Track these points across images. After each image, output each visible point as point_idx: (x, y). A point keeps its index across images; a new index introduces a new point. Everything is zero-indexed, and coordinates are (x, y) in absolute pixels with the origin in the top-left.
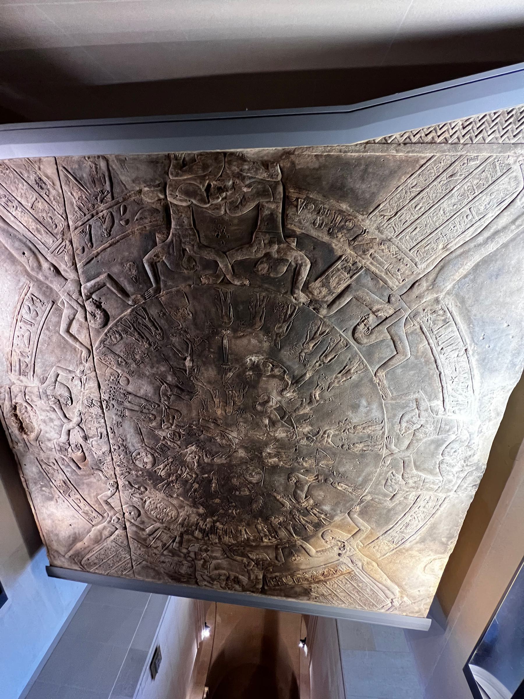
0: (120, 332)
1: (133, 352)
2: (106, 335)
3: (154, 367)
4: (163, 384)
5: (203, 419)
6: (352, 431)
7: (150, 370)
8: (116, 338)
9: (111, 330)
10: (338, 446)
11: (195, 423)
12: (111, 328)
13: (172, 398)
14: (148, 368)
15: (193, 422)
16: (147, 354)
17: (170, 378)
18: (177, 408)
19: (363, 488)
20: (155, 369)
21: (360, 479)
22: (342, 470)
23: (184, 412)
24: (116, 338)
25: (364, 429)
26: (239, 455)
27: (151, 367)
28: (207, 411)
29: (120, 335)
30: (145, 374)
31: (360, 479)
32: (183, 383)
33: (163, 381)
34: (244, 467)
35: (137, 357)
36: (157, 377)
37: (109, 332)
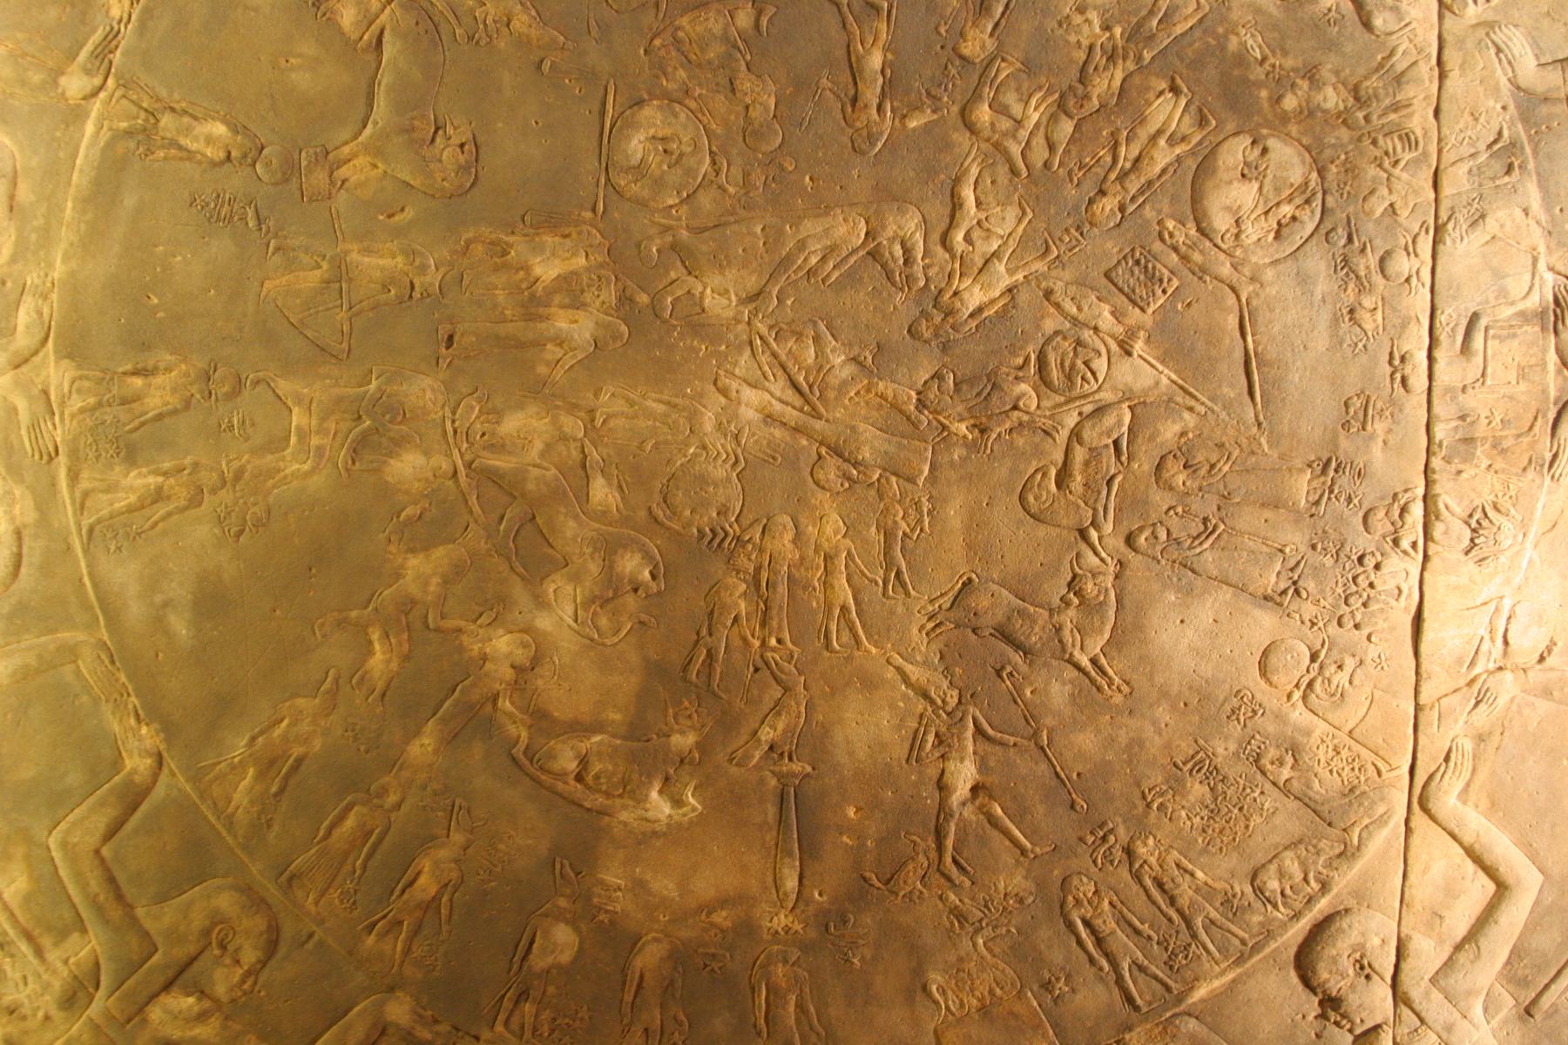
0: (1258, 905)
1: (1214, 814)
2: (1325, 887)
3: (1129, 746)
4: (1094, 661)
5: (911, 480)
6: (208, 478)
7: (1149, 731)
8: (1281, 874)
9: (1298, 906)
10: (257, 383)
11: (957, 453)
12: (1297, 916)
13: (1056, 589)
14: (1155, 743)
15: (964, 460)
16: (1148, 806)
17: (1057, 691)
18: (1042, 531)
19: (110, 145)
20: (1123, 737)
21: (130, 201)
22: (221, 246)
23: (1004, 518)
24: (1281, 874)
25: (159, 489)
26: (731, 274)
27: (1141, 744)
28: (889, 536)
29: (1259, 891)
30: (1174, 707)
31: (130, 201)
32: (998, 673)
33: (1091, 678)
34: (706, 200)
35: (1197, 790)
36: (1118, 699)
37: (1310, 900)
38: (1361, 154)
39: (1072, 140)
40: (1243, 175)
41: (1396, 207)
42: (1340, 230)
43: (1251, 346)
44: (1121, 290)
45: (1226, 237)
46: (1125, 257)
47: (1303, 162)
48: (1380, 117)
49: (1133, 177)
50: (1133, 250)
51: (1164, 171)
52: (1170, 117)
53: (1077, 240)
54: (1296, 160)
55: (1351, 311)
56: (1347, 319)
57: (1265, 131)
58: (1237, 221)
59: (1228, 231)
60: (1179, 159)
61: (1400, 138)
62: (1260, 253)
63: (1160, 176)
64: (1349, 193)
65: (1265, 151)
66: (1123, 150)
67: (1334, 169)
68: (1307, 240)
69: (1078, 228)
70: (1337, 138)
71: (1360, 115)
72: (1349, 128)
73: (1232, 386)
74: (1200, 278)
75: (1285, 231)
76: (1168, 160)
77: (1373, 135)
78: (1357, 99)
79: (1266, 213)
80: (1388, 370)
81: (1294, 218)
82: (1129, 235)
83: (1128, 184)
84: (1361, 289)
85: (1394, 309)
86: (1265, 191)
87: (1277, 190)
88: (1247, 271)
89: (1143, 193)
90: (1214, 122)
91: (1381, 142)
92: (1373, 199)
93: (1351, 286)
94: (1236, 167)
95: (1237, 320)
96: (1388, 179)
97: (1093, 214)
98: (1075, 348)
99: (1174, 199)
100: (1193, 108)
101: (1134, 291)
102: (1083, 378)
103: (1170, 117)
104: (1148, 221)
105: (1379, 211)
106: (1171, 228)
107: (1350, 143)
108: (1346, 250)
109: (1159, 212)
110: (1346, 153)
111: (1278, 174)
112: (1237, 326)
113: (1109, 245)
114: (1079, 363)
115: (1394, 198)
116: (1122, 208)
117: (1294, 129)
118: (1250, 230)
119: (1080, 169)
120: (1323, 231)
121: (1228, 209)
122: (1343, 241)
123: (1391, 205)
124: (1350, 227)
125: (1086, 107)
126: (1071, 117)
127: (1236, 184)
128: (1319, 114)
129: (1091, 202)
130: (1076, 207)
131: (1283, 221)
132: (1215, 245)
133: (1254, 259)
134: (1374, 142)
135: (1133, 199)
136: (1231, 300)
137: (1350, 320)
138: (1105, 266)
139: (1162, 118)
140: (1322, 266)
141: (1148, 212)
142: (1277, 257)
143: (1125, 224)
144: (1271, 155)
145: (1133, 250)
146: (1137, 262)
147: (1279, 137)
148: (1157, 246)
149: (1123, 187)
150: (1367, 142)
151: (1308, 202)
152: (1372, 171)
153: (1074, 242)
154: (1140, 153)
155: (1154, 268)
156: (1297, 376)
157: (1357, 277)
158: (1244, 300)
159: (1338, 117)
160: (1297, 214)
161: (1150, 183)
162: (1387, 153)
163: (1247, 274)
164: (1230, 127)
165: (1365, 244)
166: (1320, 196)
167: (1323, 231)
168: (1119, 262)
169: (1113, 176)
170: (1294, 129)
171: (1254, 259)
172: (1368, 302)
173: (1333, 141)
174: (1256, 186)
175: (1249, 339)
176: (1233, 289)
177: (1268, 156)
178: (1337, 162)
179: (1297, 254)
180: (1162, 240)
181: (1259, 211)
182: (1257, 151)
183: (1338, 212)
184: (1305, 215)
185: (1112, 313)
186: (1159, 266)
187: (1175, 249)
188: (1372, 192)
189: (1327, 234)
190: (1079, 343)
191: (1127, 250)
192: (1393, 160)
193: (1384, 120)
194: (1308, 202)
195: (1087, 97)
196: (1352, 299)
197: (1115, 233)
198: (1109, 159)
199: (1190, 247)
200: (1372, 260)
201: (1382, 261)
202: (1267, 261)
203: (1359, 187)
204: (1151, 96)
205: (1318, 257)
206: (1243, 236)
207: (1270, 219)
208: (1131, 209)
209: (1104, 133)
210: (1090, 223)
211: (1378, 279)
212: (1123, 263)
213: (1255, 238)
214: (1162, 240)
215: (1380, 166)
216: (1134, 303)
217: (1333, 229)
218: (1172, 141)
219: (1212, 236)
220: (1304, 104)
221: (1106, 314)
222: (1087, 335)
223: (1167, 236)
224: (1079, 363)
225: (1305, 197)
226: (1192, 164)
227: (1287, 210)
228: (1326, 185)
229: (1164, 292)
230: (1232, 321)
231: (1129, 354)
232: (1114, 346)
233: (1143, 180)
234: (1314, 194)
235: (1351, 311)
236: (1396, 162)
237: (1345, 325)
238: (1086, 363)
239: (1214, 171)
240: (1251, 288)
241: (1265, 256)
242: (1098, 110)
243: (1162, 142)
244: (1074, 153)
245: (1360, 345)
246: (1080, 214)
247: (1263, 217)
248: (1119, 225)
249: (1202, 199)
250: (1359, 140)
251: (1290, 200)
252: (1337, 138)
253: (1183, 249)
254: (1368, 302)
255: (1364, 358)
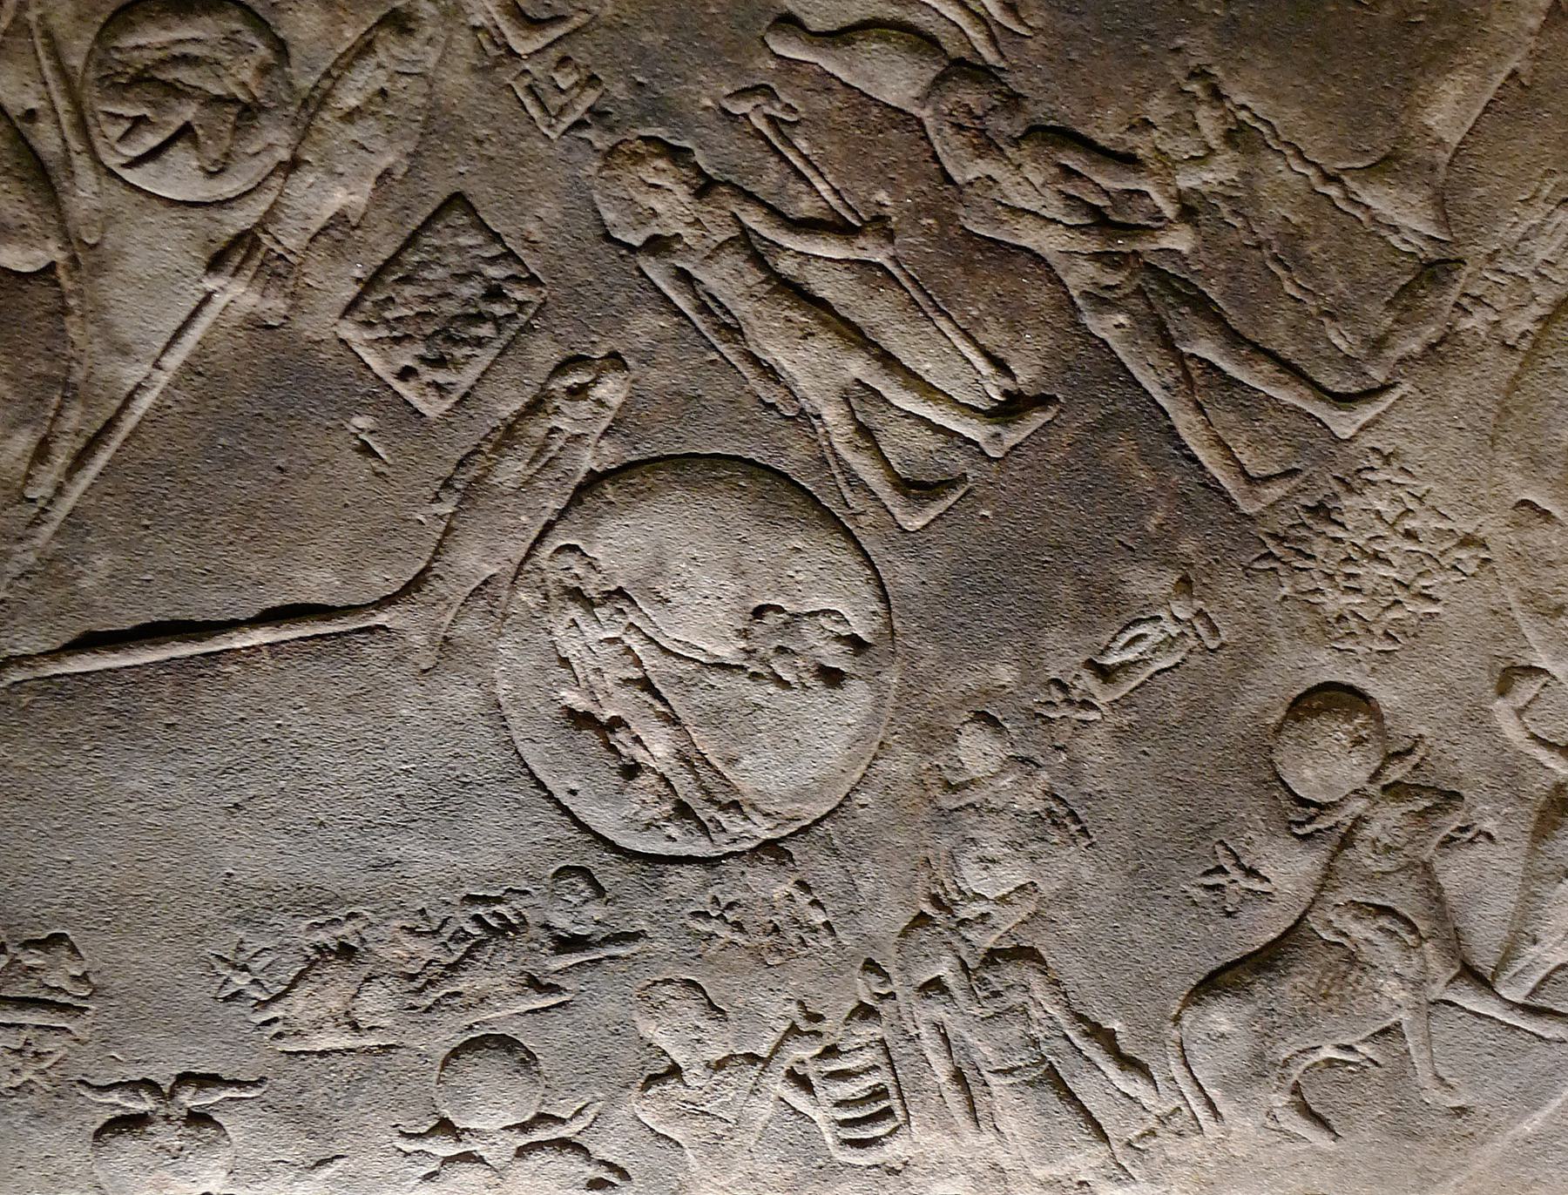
38: (832, 972)
39: (862, 100)
40: (759, 612)
41: (670, 1086)
42: (596, 911)
43: (239, 641)
44: (411, 241)
45: (570, 559)
46: (509, 255)
47: (801, 795)
48: (938, 1026)
49: (753, 277)
50: (533, 281)
51: (770, 373)
52: (929, 391)
53: (562, 110)
54: (807, 772)
55: (346, 952)
56: (321, 937)
57: (892, 677)
58: (620, 592)
59: (592, 565)
60: (805, 419)
61: (878, 1093)
62: (526, 664)
63: (755, 361)
64: (711, 936)
65: (832, 678)
66: (832, 249)
67: (781, 888)
68: (566, 811)
69: (597, 113)
70: (875, 899)
71: (945, 969)
72: (905, 933)
73: (117, 580)
74: (447, 484)
75: (589, 739)
76: (804, 383)
77: (885, 1008)
78: (993, 957)
79: (646, 684)
80: (163, 1074)
81: (631, 771)
82: (579, 271)
83: (731, 261)
84: (416, 980)
85: (355, 1083)
86: (714, 678)
87: (715, 718)
88: (471, 627)
89: (703, 308)
90: (919, 523)
91: (866, 1032)
92: (692, 1013)
93: (426, 949)
94: (782, 590)
95: (324, 599)
96: (752, 1058)
97: (637, 158)
98: (234, 100)
99: (685, 403)
100: (960, 462)
101: (407, 280)
102: (138, 121)
103: (929, 391)
104: (620, 324)
105: (650, 1029)
106: (599, 392)
107: (863, 937)
108: (534, 932)
109: (647, 359)
110: (827, 924)
111: (763, 719)
112: (301, 598)
113: (549, 209)
114: (189, 112)
115: (695, 1077)
116: (658, 245)
117: (901, 765)
118: (593, 633)
119: (771, 120)
120: (593, 859)
121: (658, 567)
122: (562, 922)
123: (675, 1071)
124: (607, 940)
125: (957, 140)
126: (923, 100)
127: (734, 587)
128: (946, 843)
129: (677, 155)
130: (659, 110)
131: (621, 735)
132: (549, 527)
133: (506, 648)
134: (865, 1012)
135: (684, 276)
136: (382, 579)
137: (320, 949)
138: (481, 192)
139: (927, 367)
140: (487, 859)
141: (646, 325)
142: (515, 718)
143: (609, 255)
144: (820, 696)
145: (533, 281)
146: (494, 293)
147: (875, 718)
148: (544, 352)
149: (721, 246)
150: (864, 989)
151: (683, 811)
152: (779, 1011)
153: (555, 101)
154: (823, 304)
155: (479, 342)
156: (146, 786)
157: (453, 967)
158: (381, 618)
159: (935, 900)
160: (644, 780)
161: (733, 331)
162: (831, 1052)
163: (462, 629)
164: (903, 574)
165: (553, 989)
166: (701, 848)
167: (593, 859)
168: (496, 238)
169: (753, 219)
170: (901, 765)
171: (506, 648)
172: (376, 1003)
173: (866, 887)
174: (727, 652)
175: (261, 636)
176: (415, 584)
177: (818, 685)
178: (803, 900)
179: (524, 782)
180: (561, 369)
181: (652, 663)
182: (834, 656)
183: (653, 905)
184: (643, 800)
185: (340, 218)
186: (485, 357)
187: (535, 407)
188: (714, 1011)
189: (584, 872)
190: (248, 113)
191: (533, 264)
192: (811, 1071)
193: (929, 1042)
194: (683, 811)
195: (986, 145)
196: (385, 952)
197: (585, 223)
198: (805, 207)
199: (541, 452)
200: (504, 1016)
201: (507, 1044)
202: (502, 689)
203: (730, 968)
204: (992, 337)
205: (516, 846)
206: (575, 612)
207: (624, 694)
208: (655, 270)
209: (882, 196)
210: (614, 149)
211: (448, 1032)
212: (496, 250)
213: (570, 649)
214: (561, 369)
215: (794, 1030)
216: (370, 284)
217: (600, 891)
218: (858, 395)
219: (574, 516)
220: (972, 796)
221: (339, 198)
222: (275, 138)
223: (573, 380)
224: (189, 112)
225: (695, 800)
226: (793, 458)
227: (659, 748)
228: (733, 866)
229: (406, 374)
230: (316, 585)
231: (215, 264)
232: (241, 219)
233: (743, 309)
234: (703, 828)
235: (346, 952)
236: (803, 1083)
237: (305, 935)
238: (185, 132)
239: (771, 521)
240: (418, 639)
241: (516, 684)
242: (948, 179)
243: (857, 367)
244: (822, 103)
245: (241, 981)
246: (642, 120)
247: (635, 673)
248: (607, 237)
249: (687, 484)
250: (871, 966)
251: (687, 760)
252: (875, 899)
253: (536, 430)
254: (376, 1003)
255: (199, 992)
